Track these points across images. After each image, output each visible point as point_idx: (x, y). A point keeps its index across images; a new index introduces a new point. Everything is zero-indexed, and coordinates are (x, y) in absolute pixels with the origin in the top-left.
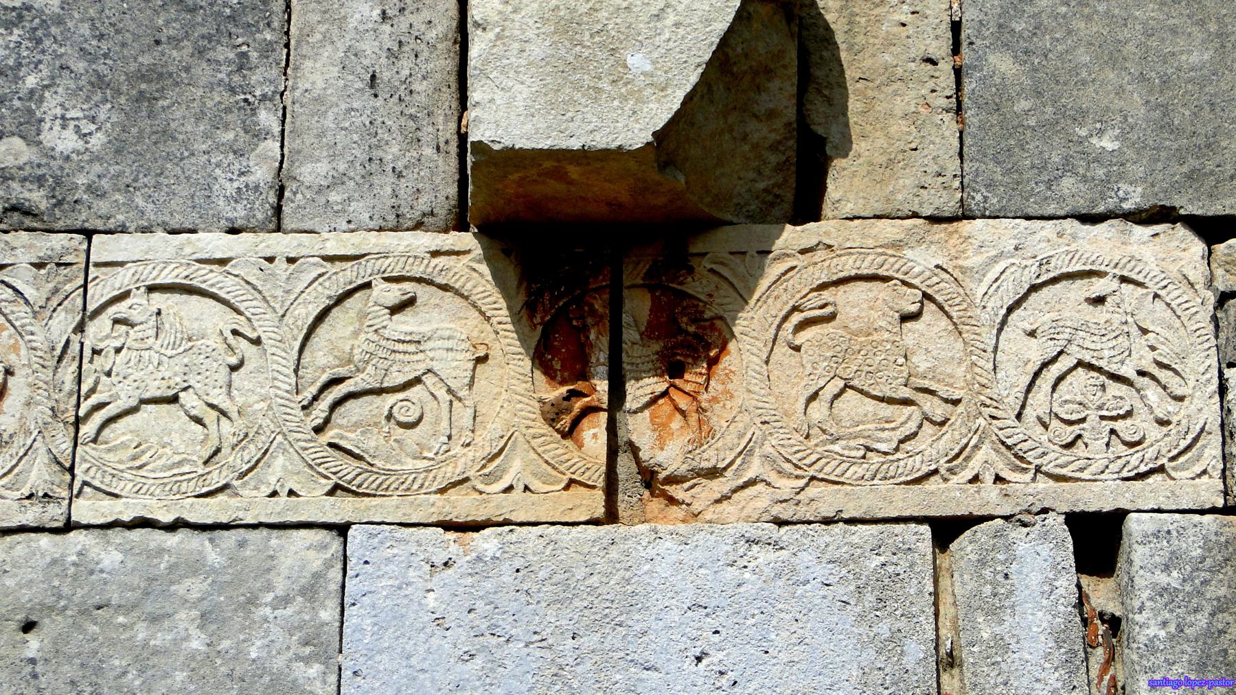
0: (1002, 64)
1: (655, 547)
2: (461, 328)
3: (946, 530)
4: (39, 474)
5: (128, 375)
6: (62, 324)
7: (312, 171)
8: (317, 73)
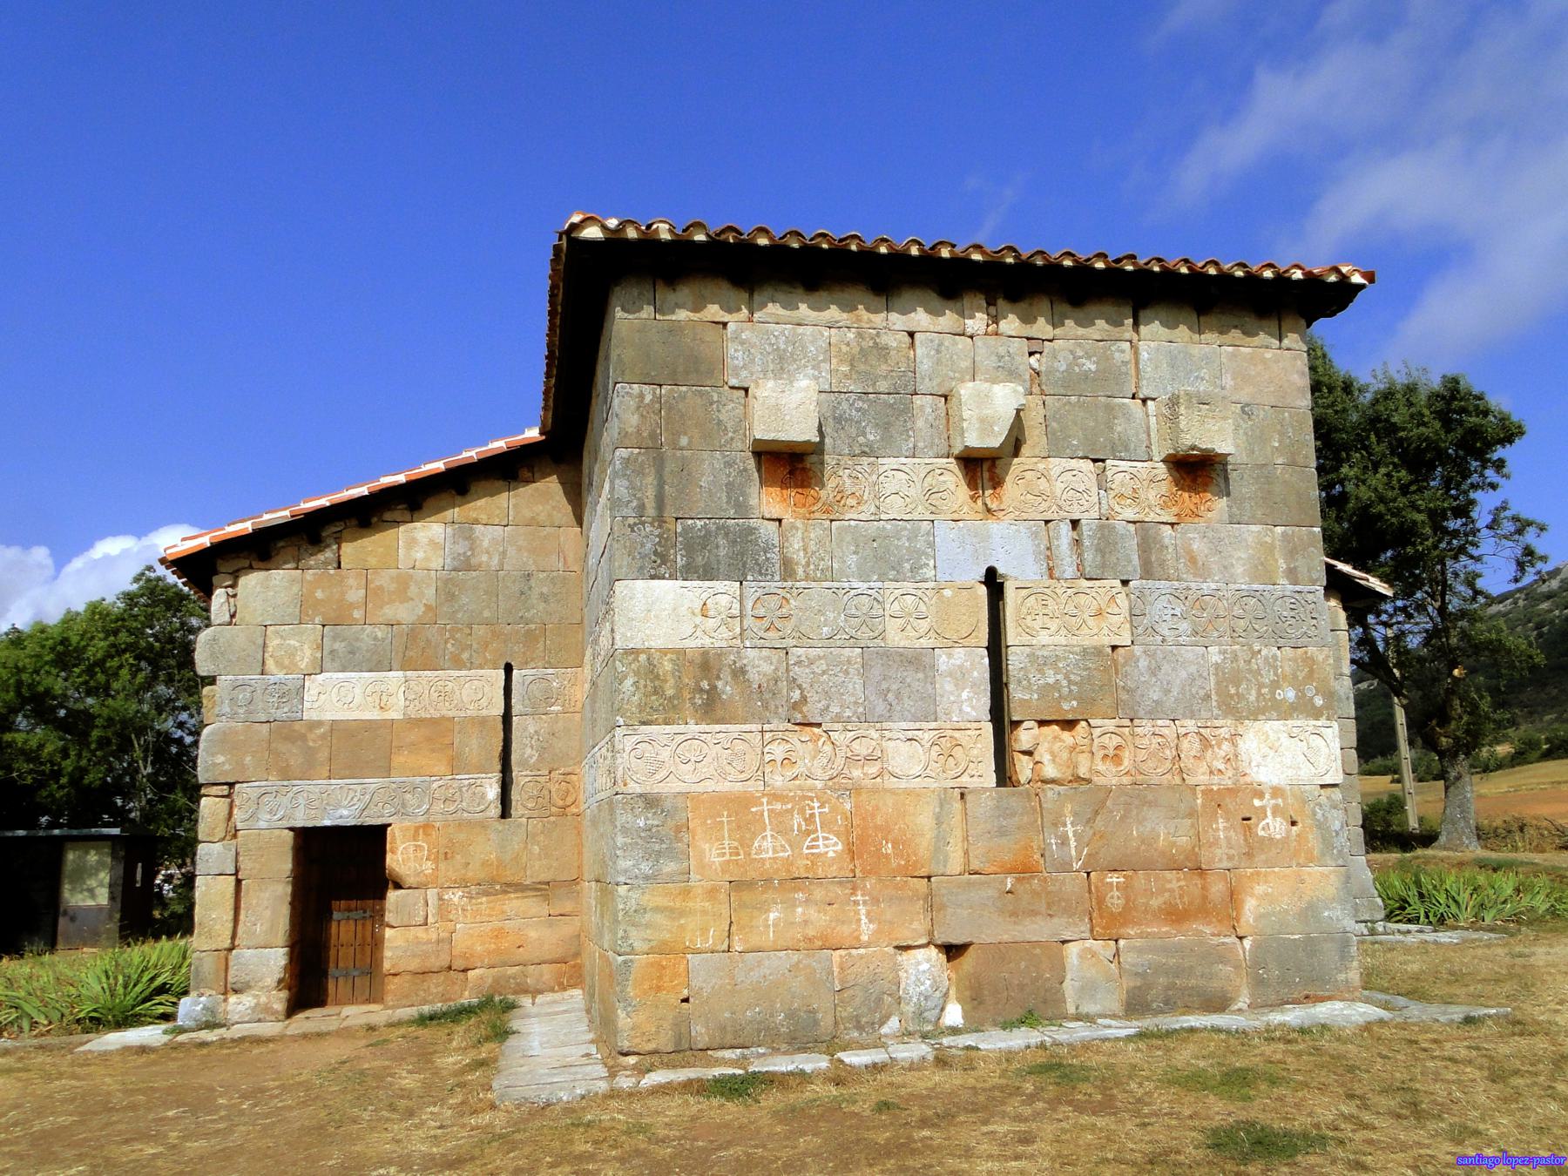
0: (1054, 425)
1: (993, 526)
2: (953, 479)
3: (1047, 522)
4: (873, 509)
5: (889, 488)
6: (874, 477)
7: (921, 445)
8: (920, 423)
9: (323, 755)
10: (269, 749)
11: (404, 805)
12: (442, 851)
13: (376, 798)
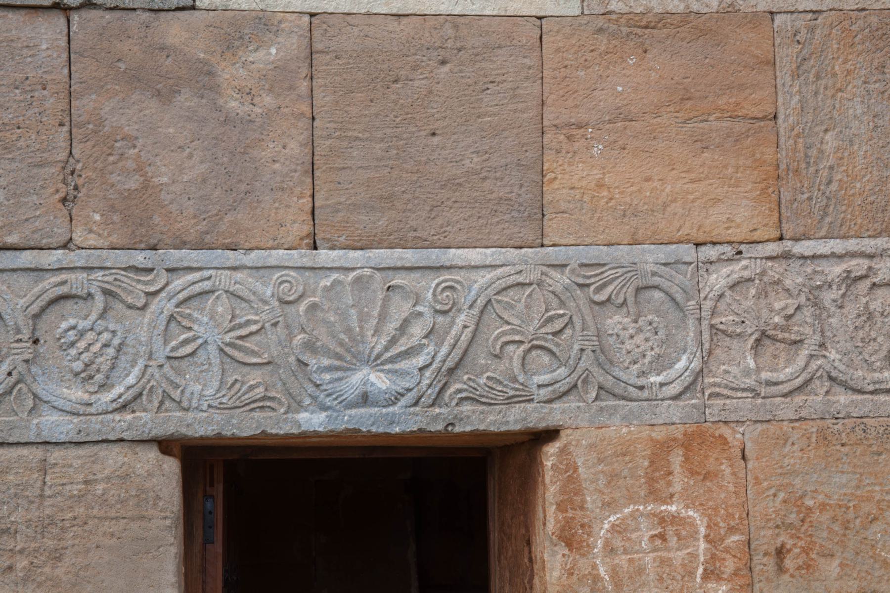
9: (283, 150)
10: (68, 120)
11: (603, 355)
12: (765, 539)
13: (495, 332)
